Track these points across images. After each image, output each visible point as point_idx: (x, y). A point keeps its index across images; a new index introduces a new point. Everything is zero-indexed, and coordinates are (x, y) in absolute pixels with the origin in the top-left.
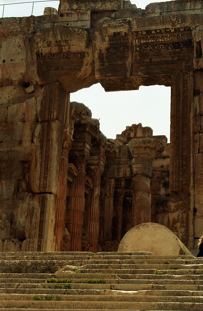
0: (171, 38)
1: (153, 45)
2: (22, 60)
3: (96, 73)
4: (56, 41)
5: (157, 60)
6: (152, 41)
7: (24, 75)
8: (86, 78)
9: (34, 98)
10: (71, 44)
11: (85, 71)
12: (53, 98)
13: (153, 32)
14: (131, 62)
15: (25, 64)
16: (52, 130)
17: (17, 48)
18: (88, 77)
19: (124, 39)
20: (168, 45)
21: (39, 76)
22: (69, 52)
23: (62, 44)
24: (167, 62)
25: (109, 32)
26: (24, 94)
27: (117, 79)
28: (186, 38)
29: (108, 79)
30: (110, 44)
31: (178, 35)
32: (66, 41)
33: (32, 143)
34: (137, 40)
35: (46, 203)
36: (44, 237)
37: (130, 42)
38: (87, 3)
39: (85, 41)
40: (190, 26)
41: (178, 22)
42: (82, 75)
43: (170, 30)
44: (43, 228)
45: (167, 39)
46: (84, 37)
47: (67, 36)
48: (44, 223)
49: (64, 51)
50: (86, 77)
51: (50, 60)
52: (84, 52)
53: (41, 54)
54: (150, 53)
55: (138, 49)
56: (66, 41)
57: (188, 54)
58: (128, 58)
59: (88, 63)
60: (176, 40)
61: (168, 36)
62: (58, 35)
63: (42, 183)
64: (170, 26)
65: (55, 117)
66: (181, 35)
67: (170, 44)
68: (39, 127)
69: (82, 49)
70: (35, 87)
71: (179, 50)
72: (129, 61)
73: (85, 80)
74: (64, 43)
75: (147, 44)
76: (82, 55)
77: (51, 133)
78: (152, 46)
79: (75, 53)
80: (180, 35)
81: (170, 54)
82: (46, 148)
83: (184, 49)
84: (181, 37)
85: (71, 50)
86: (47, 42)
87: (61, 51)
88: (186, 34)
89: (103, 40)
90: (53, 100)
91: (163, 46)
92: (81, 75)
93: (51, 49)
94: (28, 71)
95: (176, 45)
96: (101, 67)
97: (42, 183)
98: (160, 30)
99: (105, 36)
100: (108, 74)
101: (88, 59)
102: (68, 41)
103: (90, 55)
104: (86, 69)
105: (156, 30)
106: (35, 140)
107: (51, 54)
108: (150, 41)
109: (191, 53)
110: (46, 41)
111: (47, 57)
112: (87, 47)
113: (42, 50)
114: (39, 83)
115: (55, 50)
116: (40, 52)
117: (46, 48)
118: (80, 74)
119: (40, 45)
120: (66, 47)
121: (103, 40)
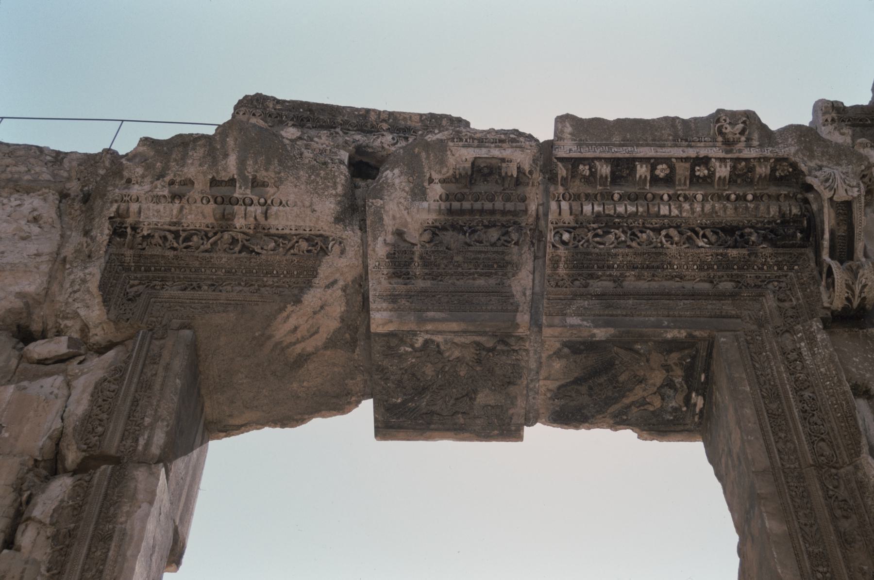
0: (708, 207)
1: (631, 227)
2: (38, 255)
3: (372, 306)
4: (214, 182)
5: (643, 285)
6: (631, 209)
7: (30, 303)
8: (309, 355)
9: (59, 380)
10: (277, 197)
11: (315, 313)
12: (159, 380)
13: (642, 170)
14: (531, 284)
15: (45, 268)
16: (133, 498)
17: (23, 222)
18: (317, 350)
19: (508, 199)
20: (697, 234)
21: (106, 301)
22: (261, 231)
23: (236, 195)
24: (694, 295)
25: (451, 161)
26: (14, 362)
27: (463, 346)
28: (774, 210)
29: (419, 342)
30: (450, 211)
31: (738, 197)
32: (256, 184)
33: (10, 548)
34: (565, 205)
37: (533, 208)
38: (338, 130)
39: (336, 195)
40: (798, 160)
41: (748, 140)
42: (299, 335)
43: (712, 174)
45: (693, 211)
46: (335, 183)
47: (268, 162)
49: (239, 223)
50: (309, 346)
51: (171, 254)
52: (325, 239)
53: (134, 228)
54: (616, 255)
55: (566, 236)
56: (256, 184)
57: (780, 273)
58: (517, 267)
59: (335, 282)
60: (728, 214)
61: (699, 197)
62: (226, 156)
64: (715, 152)
65: (155, 450)
66: (755, 197)
67: (703, 228)
68: (60, 487)
69: (321, 224)
70: (72, 342)
71: (745, 252)
72: (523, 282)
73: (302, 359)
74: (248, 191)
75: (606, 223)
76: (319, 245)
77: (126, 508)
78: (624, 232)
79: (283, 237)
80: (750, 197)
81: (700, 269)
82: (83, 571)
83: (765, 249)
84: (751, 206)
85: (272, 222)
86: (172, 183)
87: (225, 221)
88: (769, 196)
89: (418, 193)
90: (157, 387)
91: (673, 232)
92: (296, 328)
93: (181, 209)
94: (55, 288)
95: (730, 234)
96: (400, 287)
98: (667, 160)
99: (431, 181)
100: (431, 314)
101: (338, 266)
102: (264, 185)
103: (351, 251)
104: (318, 311)
105: (653, 163)
106: (27, 537)
107: (177, 235)
108: (621, 209)
109: (791, 269)
110: (167, 179)
111: (157, 239)
112: (338, 220)
113: (139, 212)
114: (98, 336)
115: (199, 214)
116: (130, 220)
117: (161, 207)
118: (292, 322)
119: (135, 190)
120: (251, 209)
121: (418, 193)
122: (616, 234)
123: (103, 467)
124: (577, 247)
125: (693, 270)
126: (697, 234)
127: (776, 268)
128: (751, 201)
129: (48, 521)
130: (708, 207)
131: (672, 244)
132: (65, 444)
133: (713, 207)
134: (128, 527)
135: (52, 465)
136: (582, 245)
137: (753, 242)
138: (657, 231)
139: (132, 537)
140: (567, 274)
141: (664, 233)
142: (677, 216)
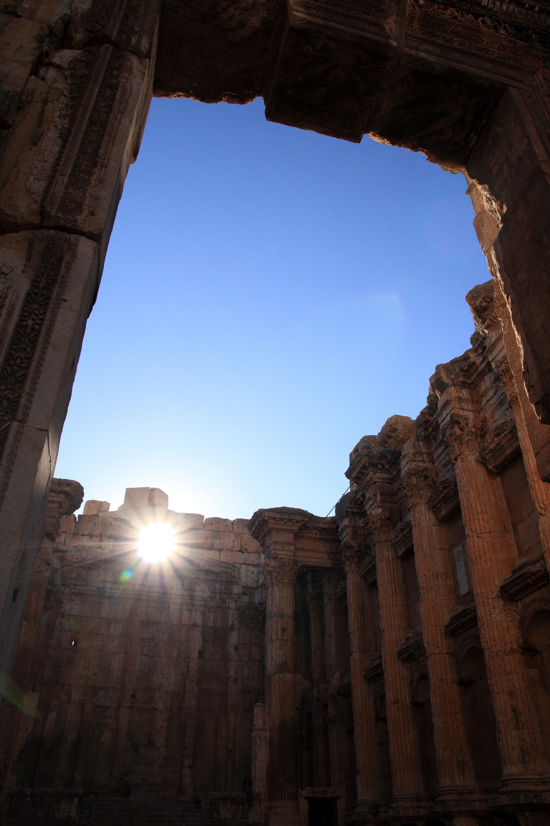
0: (511, 7)
35: (68, 268)
36: (26, 415)
44: (27, 368)
48: (39, 347)
63: (59, 190)
80: (537, 9)
84: (536, 15)
97: (59, 190)
122: (452, 11)
123: (107, 45)
124: (427, 11)
125: (495, 48)
126: (500, 25)
127: (542, 61)
128: (536, 12)
129: (66, 66)
130: (511, 7)
131: (485, 27)
132: (72, 29)
133: (514, 9)
134: (128, 85)
135: (64, 41)
136: (431, 11)
137: (533, 40)
138: (476, 17)
139: (131, 92)
140: (418, 29)
141: (480, 19)
142: (491, 9)
